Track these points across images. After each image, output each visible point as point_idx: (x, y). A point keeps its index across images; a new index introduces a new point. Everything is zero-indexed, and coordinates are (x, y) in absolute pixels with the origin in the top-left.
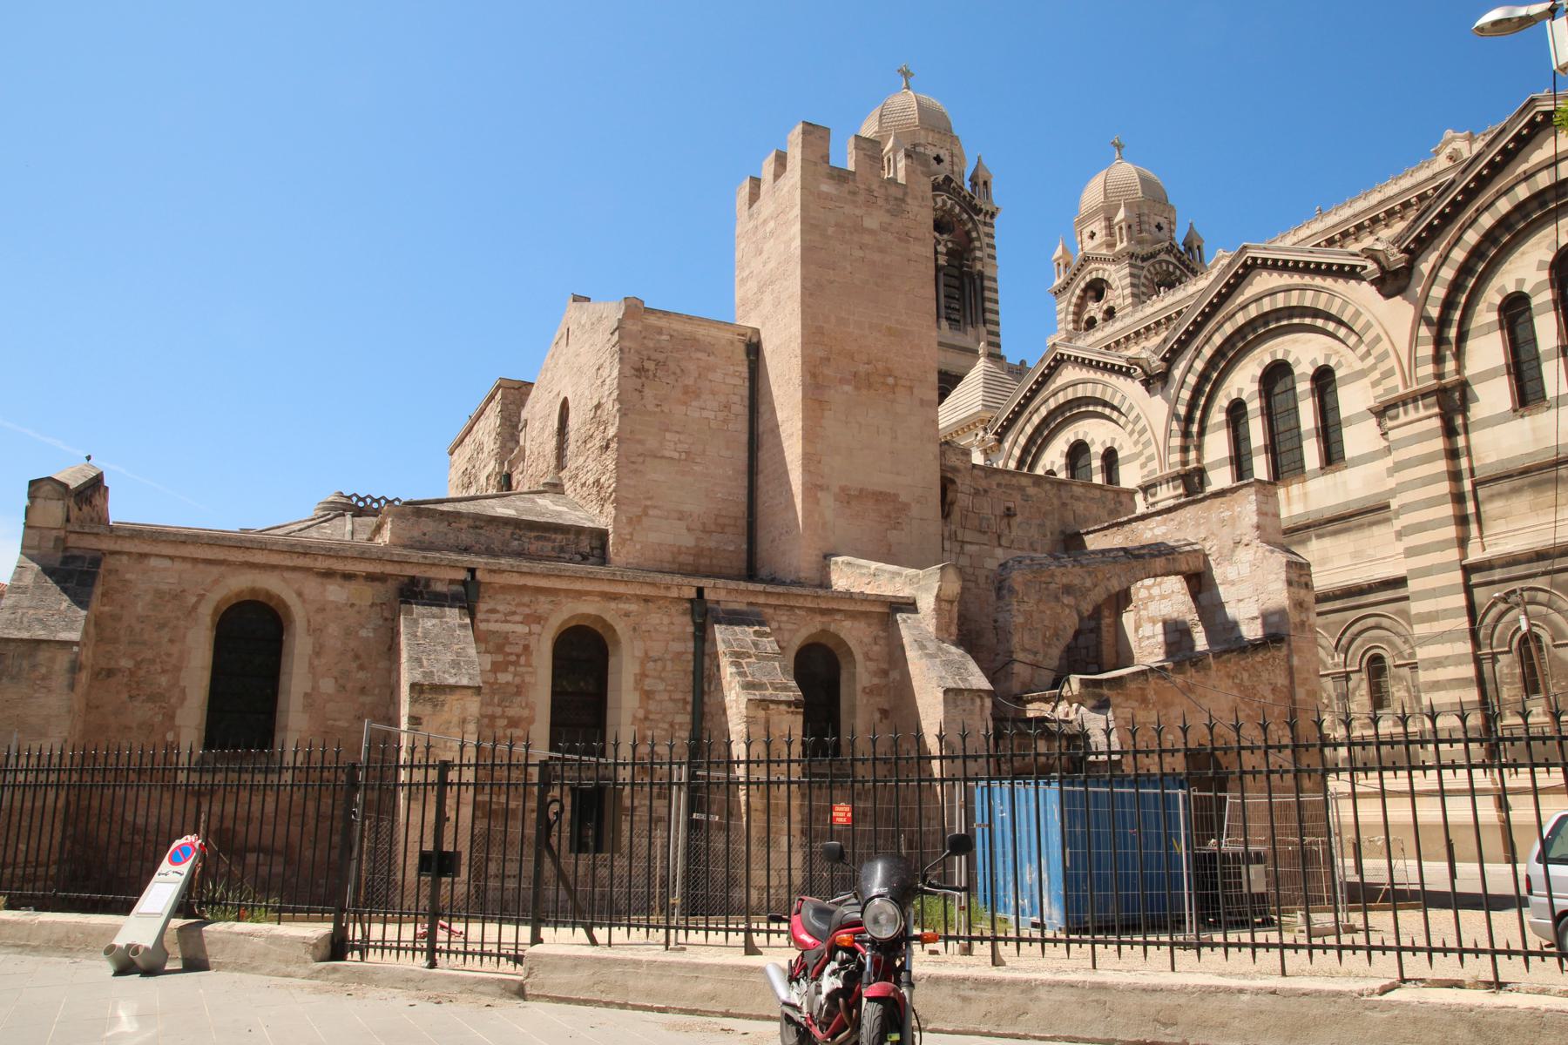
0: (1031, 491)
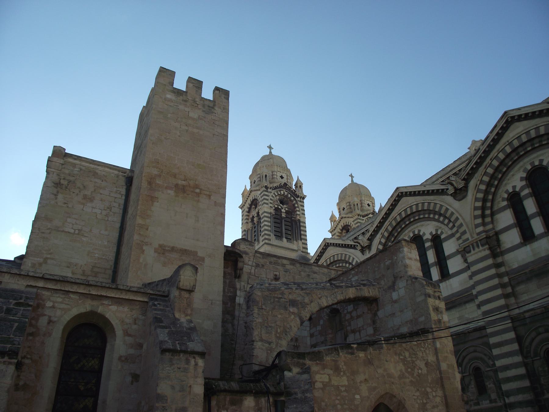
0: (289, 267)
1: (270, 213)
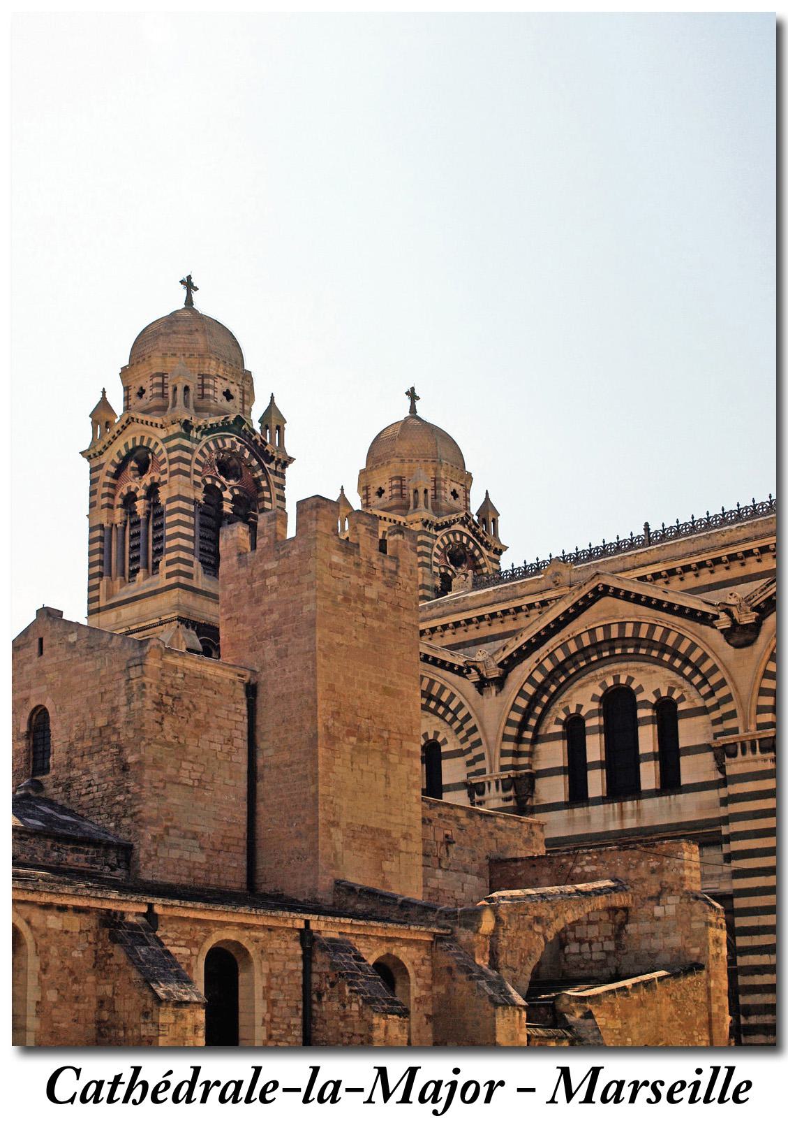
1: (195, 502)
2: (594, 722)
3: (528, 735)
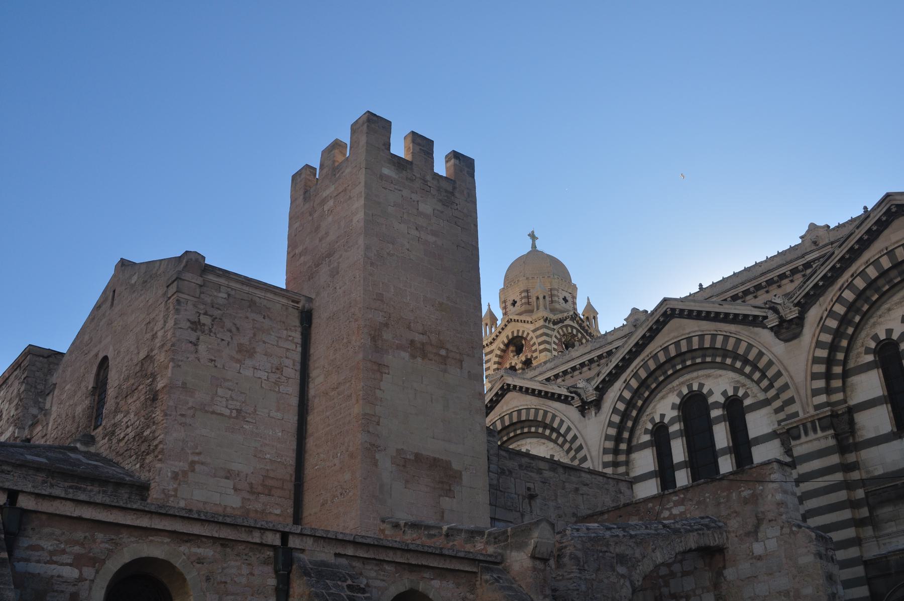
0: (547, 474)
2: (675, 428)
3: (623, 446)
